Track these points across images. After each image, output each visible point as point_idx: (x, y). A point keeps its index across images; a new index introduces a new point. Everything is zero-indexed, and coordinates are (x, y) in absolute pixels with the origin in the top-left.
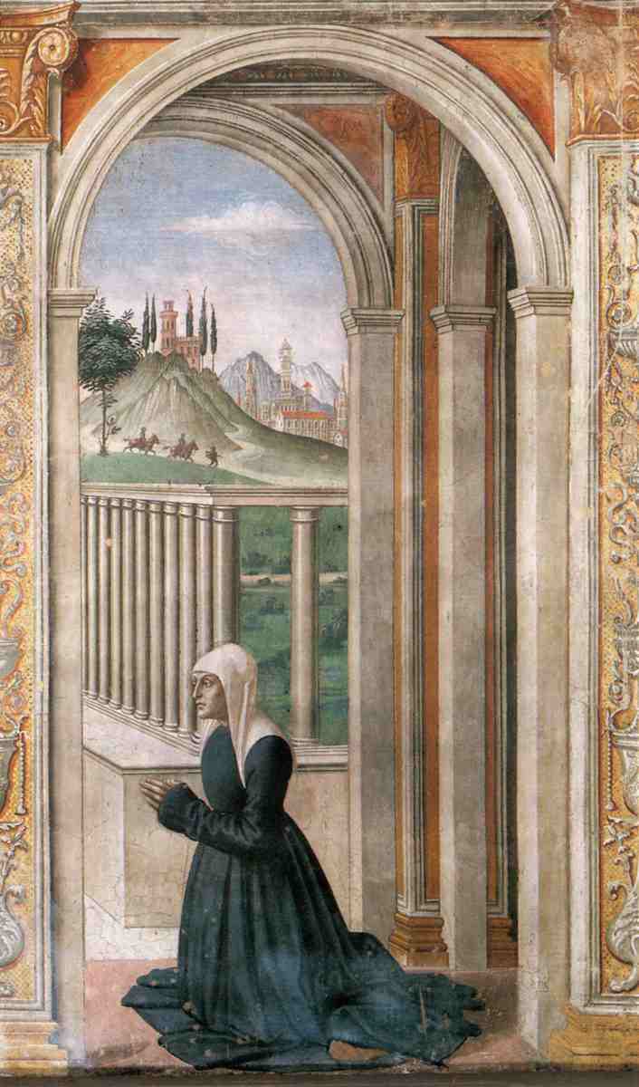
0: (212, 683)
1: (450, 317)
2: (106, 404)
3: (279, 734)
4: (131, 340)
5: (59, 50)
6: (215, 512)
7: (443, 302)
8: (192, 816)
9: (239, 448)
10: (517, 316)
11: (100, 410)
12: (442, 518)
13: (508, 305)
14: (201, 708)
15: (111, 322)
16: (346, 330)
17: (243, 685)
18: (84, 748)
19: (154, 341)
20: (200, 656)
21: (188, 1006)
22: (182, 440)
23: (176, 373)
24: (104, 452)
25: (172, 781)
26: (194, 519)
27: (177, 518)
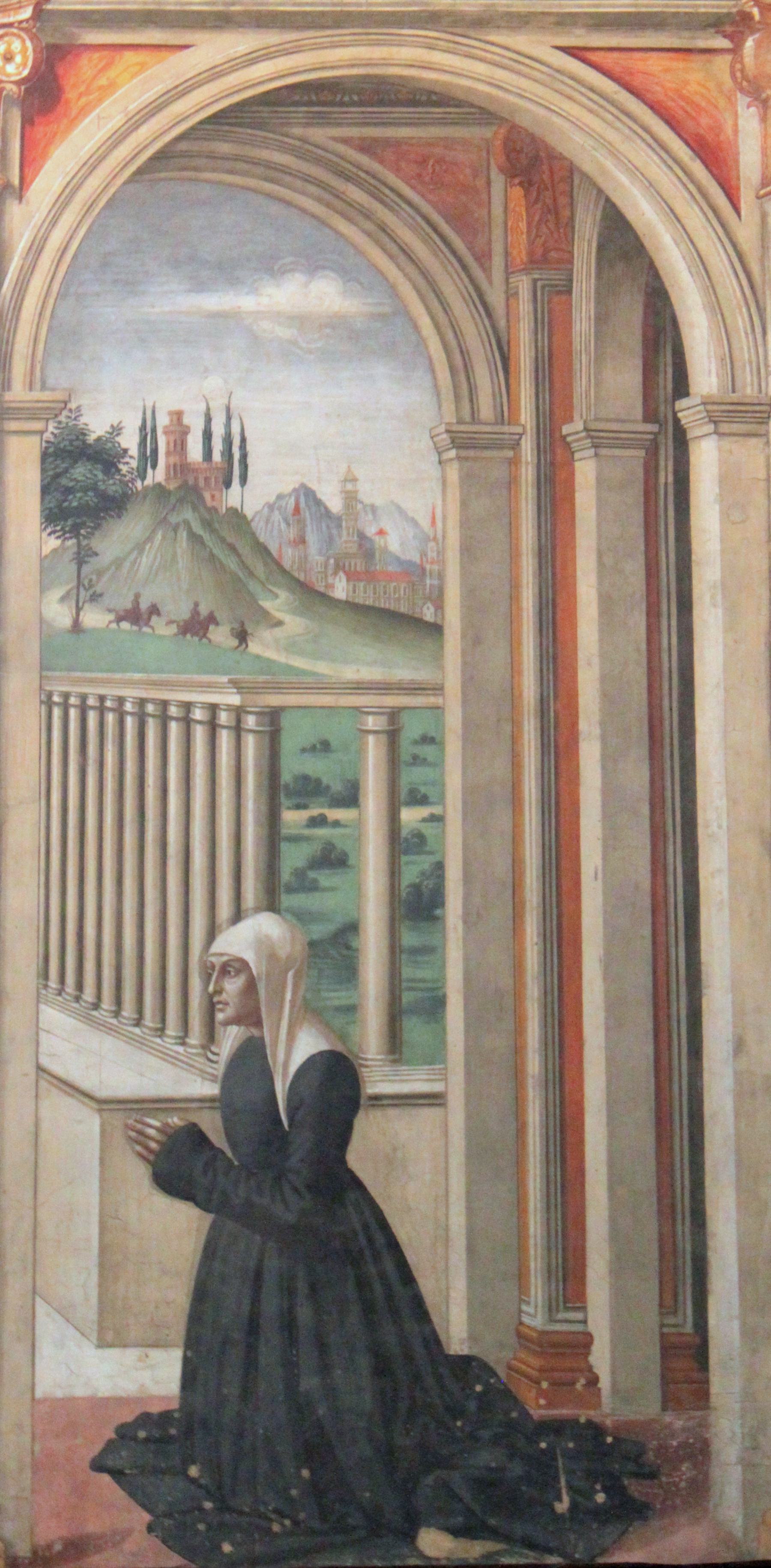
0: (238, 972)
1: (592, 437)
2: (81, 558)
3: (339, 1048)
4: (121, 466)
5: (18, 59)
6: (243, 715)
7: (581, 417)
8: (205, 1172)
9: (279, 623)
10: (690, 435)
11: (74, 567)
12: (583, 725)
13: (677, 421)
14: (221, 1010)
15: (91, 438)
16: (439, 454)
17: (286, 972)
18: (40, 1069)
19: (154, 466)
20: (221, 932)
21: (193, 1471)
22: (195, 612)
23: (188, 514)
24: (77, 627)
25: (175, 1121)
26: (213, 726)
27: (187, 722)
